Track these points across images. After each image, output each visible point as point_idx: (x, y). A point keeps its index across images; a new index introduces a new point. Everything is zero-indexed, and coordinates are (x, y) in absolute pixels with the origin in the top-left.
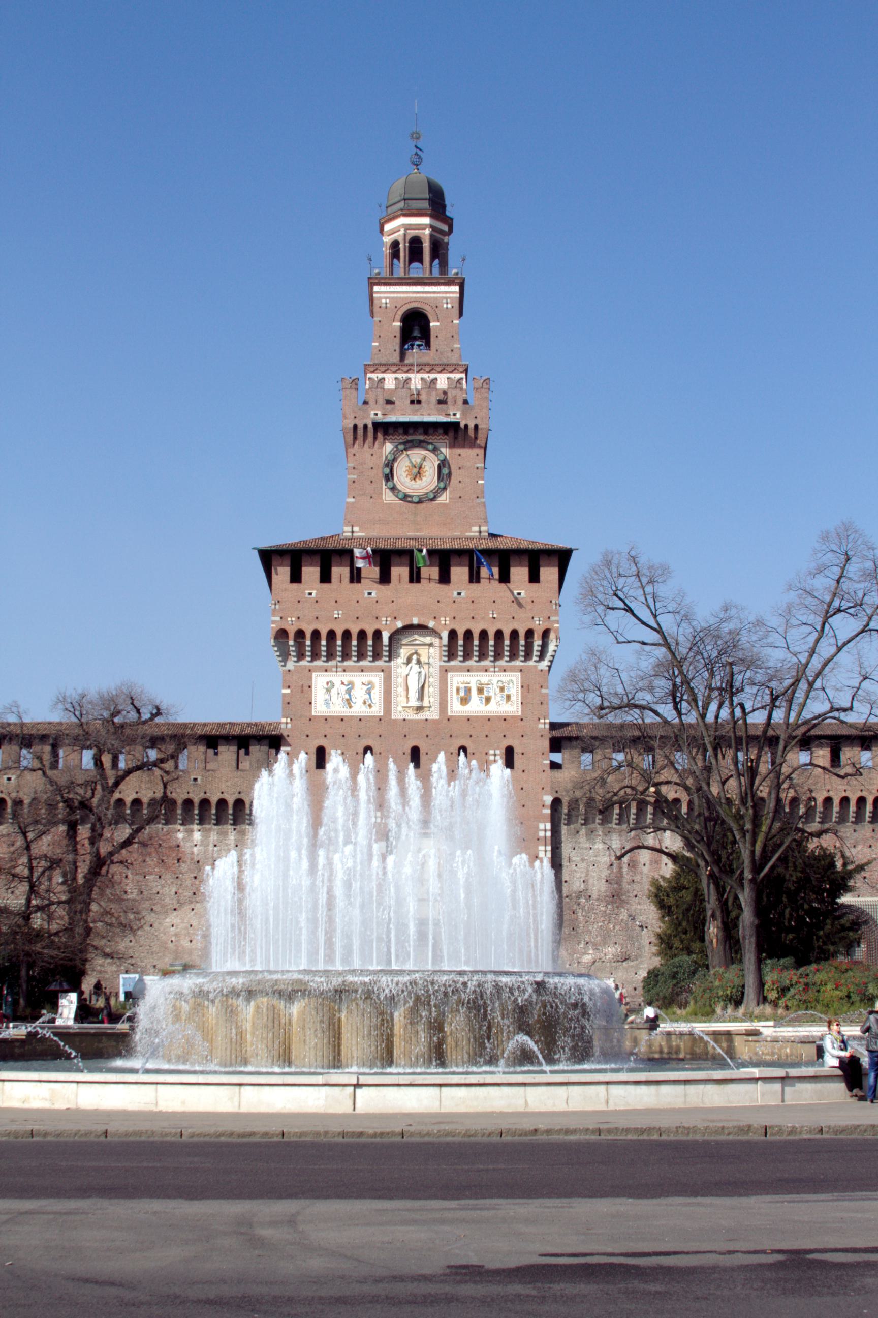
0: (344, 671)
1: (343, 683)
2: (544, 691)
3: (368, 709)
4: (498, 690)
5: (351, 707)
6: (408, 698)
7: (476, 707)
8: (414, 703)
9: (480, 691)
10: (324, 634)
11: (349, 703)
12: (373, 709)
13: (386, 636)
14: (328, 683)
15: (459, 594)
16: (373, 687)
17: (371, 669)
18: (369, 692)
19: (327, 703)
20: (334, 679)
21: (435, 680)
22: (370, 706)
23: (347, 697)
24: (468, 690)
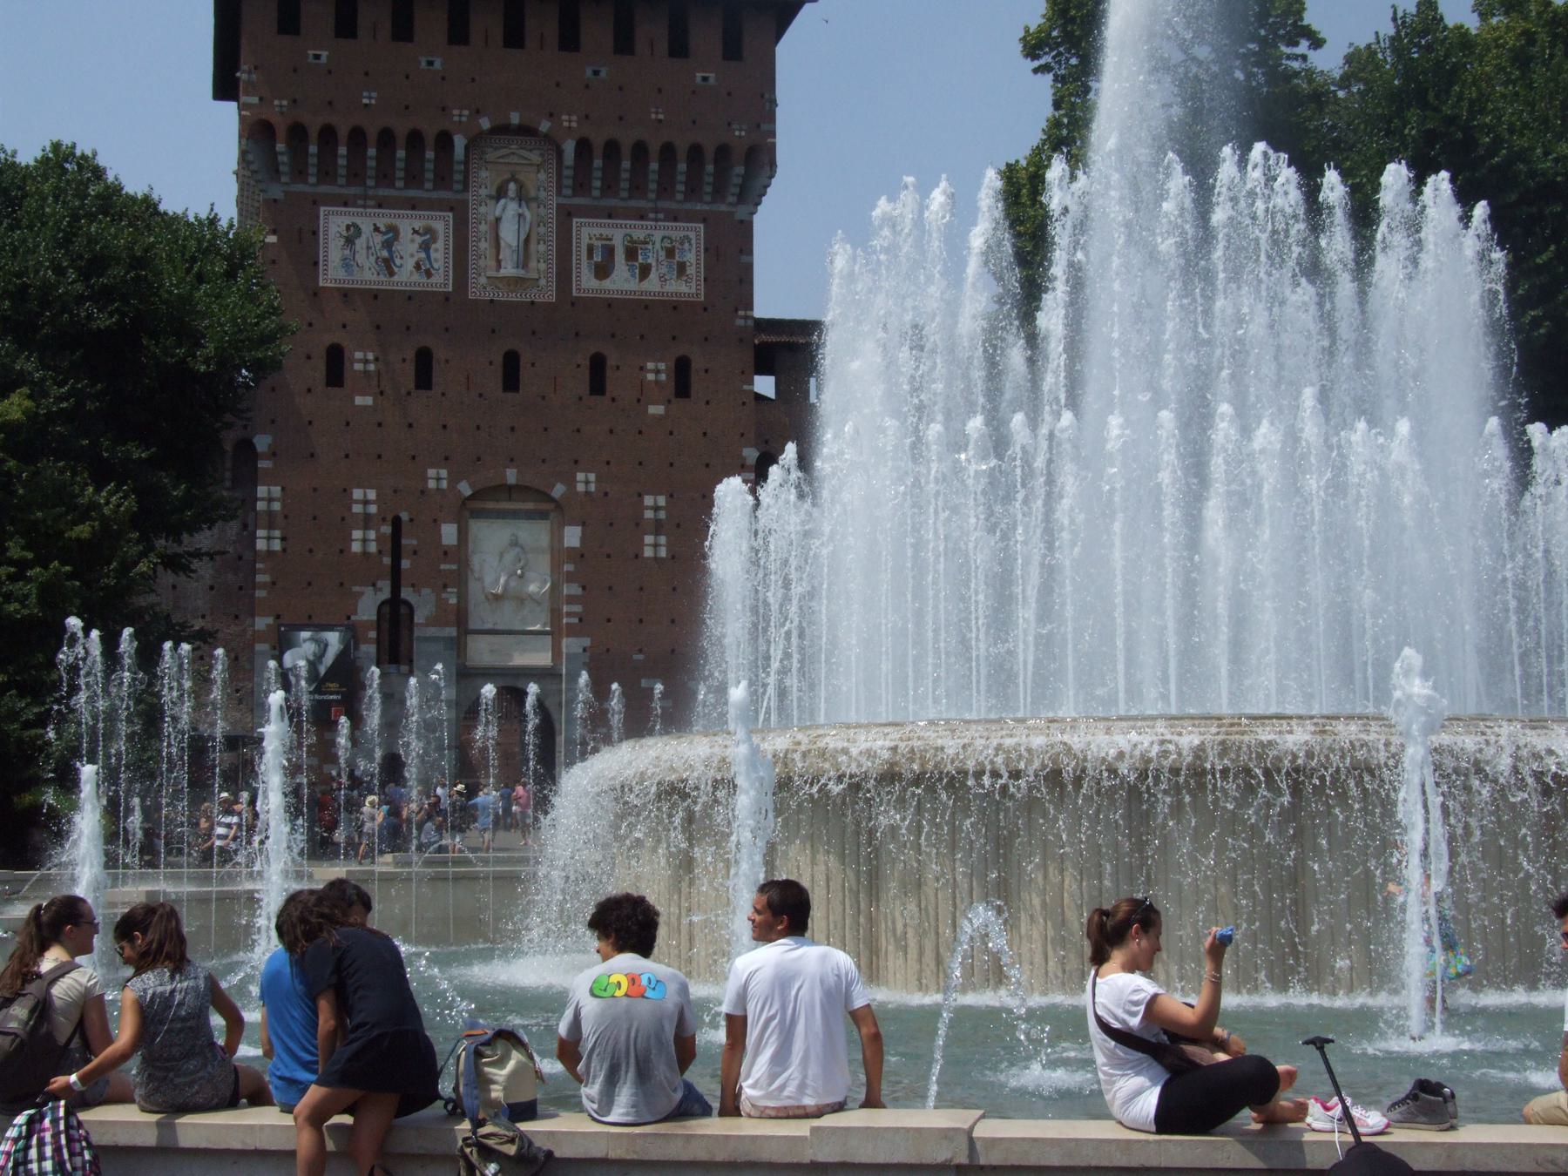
0: (380, 206)
1: (377, 229)
2: (744, 258)
3: (424, 280)
4: (662, 254)
5: (392, 274)
6: (499, 262)
7: (622, 281)
8: (508, 270)
9: (631, 254)
10: (343, 132)
11: (388, 265)
12: (433, 280)
13: (459, 142)
14: (348, 227)
15: (596, 73)
16: (435, 241)
17: (431, 205)
18: (425, 247)
19: (347, 264)
20: (358, 221)
21: (550, 230)
22: (429, 274)
23: (385, 254)
24: (609, 252)
